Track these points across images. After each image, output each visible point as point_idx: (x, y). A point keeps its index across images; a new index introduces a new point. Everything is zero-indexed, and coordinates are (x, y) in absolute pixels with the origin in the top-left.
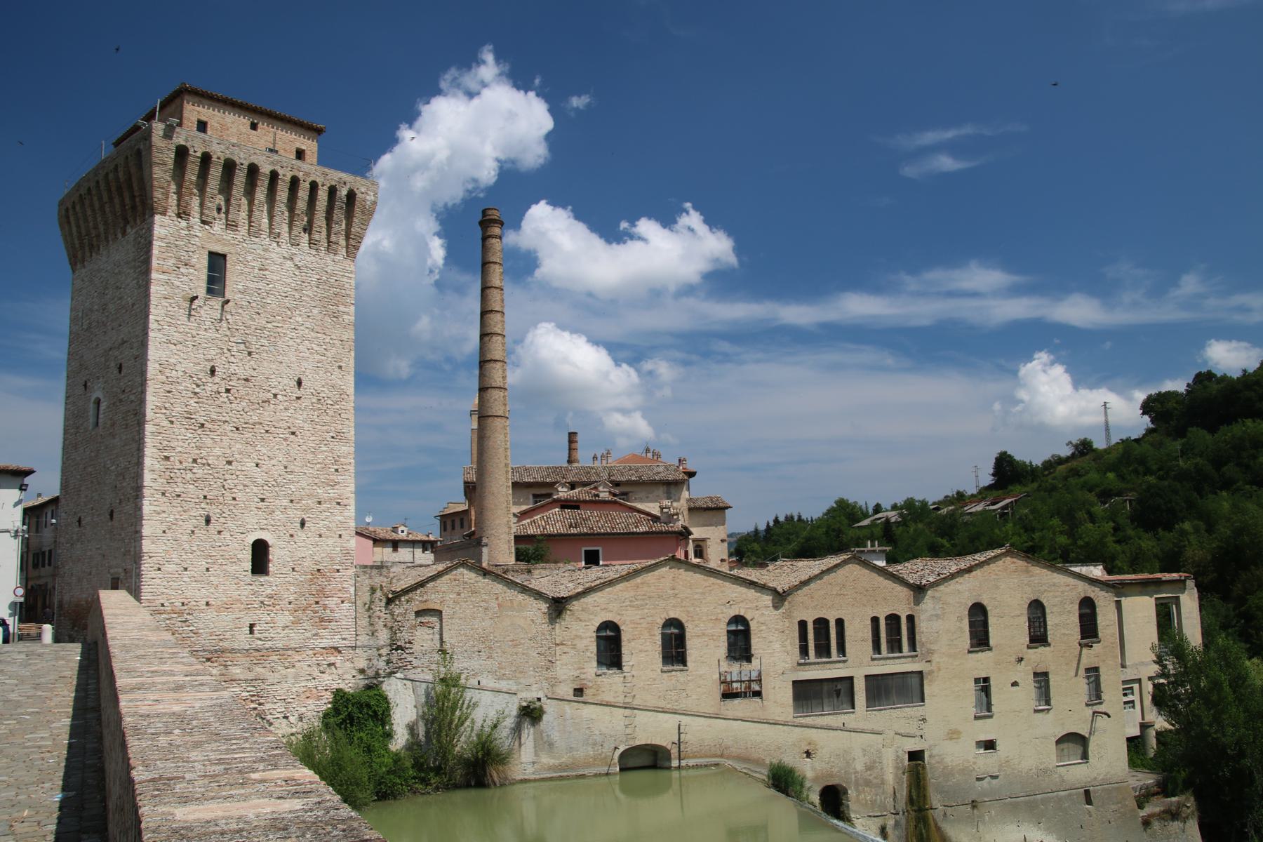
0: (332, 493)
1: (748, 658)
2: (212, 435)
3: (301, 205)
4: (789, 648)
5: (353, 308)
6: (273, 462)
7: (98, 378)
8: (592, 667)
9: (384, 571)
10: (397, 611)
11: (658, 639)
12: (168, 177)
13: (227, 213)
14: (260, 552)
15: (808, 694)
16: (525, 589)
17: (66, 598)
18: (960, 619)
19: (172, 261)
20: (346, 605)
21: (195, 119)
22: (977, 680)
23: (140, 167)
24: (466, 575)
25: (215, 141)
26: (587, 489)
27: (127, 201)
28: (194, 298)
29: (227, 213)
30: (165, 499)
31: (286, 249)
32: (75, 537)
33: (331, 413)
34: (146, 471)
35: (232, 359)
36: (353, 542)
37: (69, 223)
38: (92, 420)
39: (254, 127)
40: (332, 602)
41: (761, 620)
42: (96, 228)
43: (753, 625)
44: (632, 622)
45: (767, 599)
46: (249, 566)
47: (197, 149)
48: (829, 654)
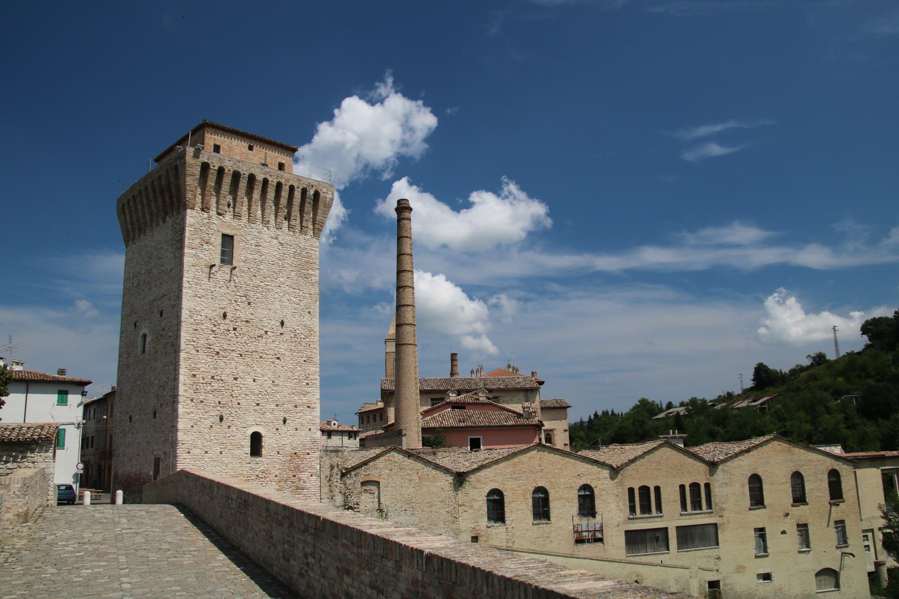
0: (305, 399)
1: (593, 515)
2: (225, 360)
3: (284, 201)
4: (622, 507)
5: (318, 271)
6: (265, 378)
7: (145, 320)
8: (484, 521)
9: (340, 454)
10: (348, 482)
11: (531, 500)
12: (196, 184)
13: (234, 207)
14: (256, 440)
15: (636, 540)
16: (437, 467)
17: (120, 471)
18: (743, 485)
19: (199, 240)
20: (314, 478)
21: (212, 144)
22: (756, 530)
23: (177, 177)
24: (396, 457)
25: (227, 159)
26: (470, 394)
27: (167, 199)
28: (212, 266)
29: (234, 207)
30: (193, 404)
31: (273, 231)
32: (127, 429)
33: (303, 344)
34: (180, 385)
35: (238, 308)
36: (319, 433)
37: (124, 213)
38: (140, 349)
39: (251, 148)
40: (304, 476)
41: (602, 487)
42: (144, 217)
43: (596, 491)
44: (512, 489)
45: (606, 473)
46: (248, 450)
47: (215, 165)
48: (650, 511)
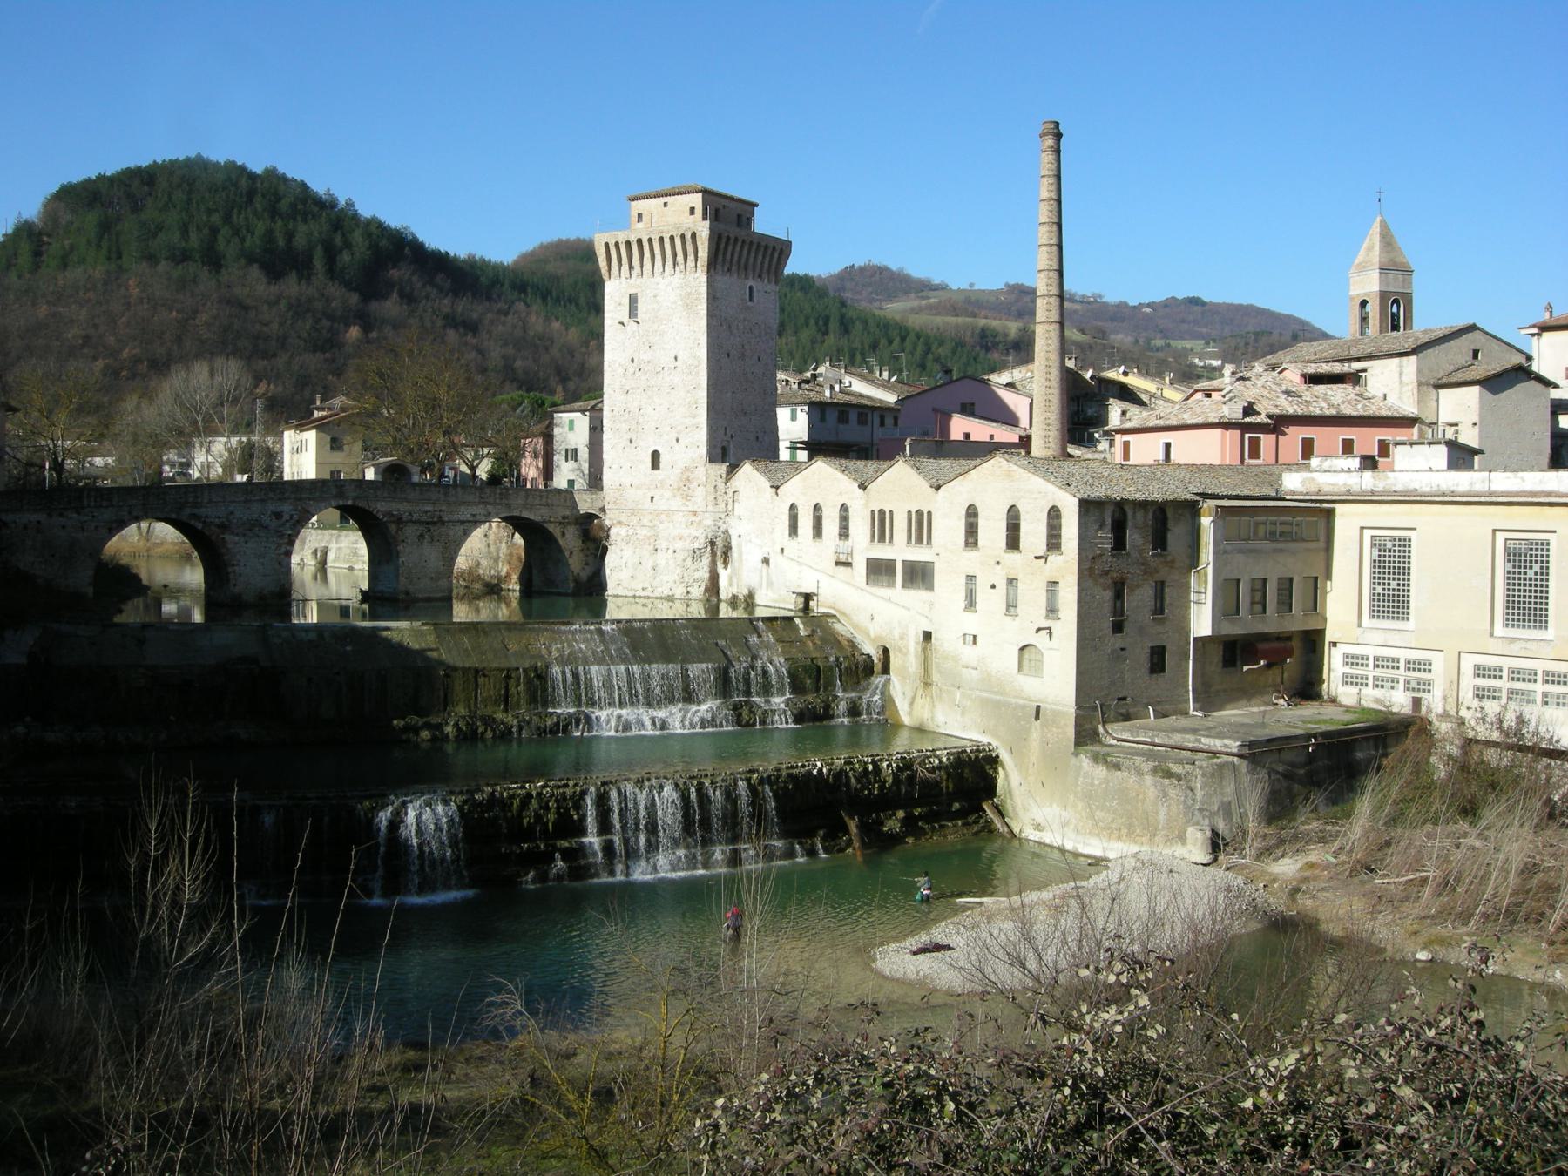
14: (655, 458)
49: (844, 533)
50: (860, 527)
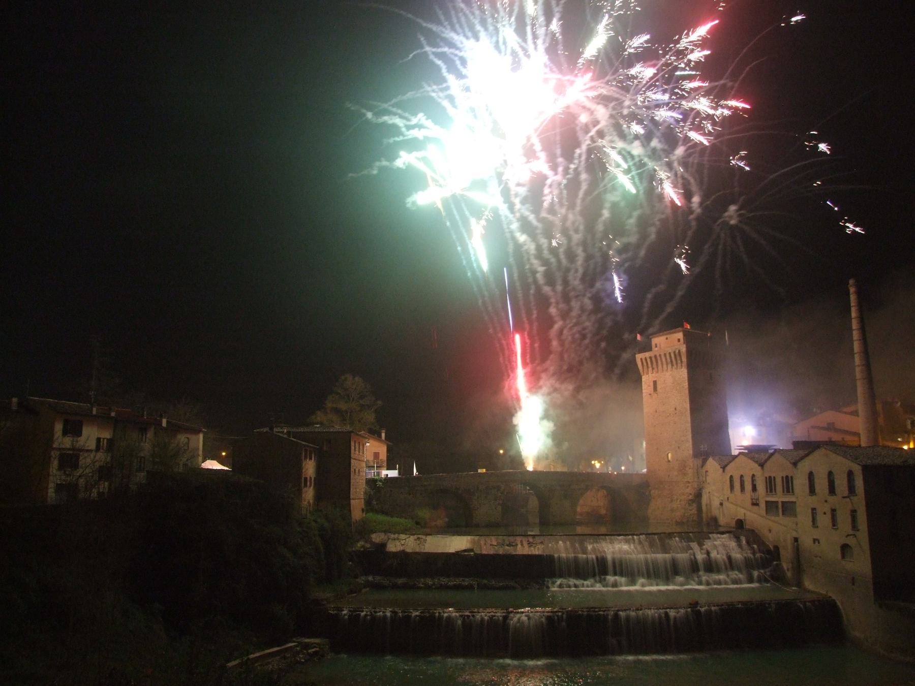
49: (754, 488)
50: (761, 487)
